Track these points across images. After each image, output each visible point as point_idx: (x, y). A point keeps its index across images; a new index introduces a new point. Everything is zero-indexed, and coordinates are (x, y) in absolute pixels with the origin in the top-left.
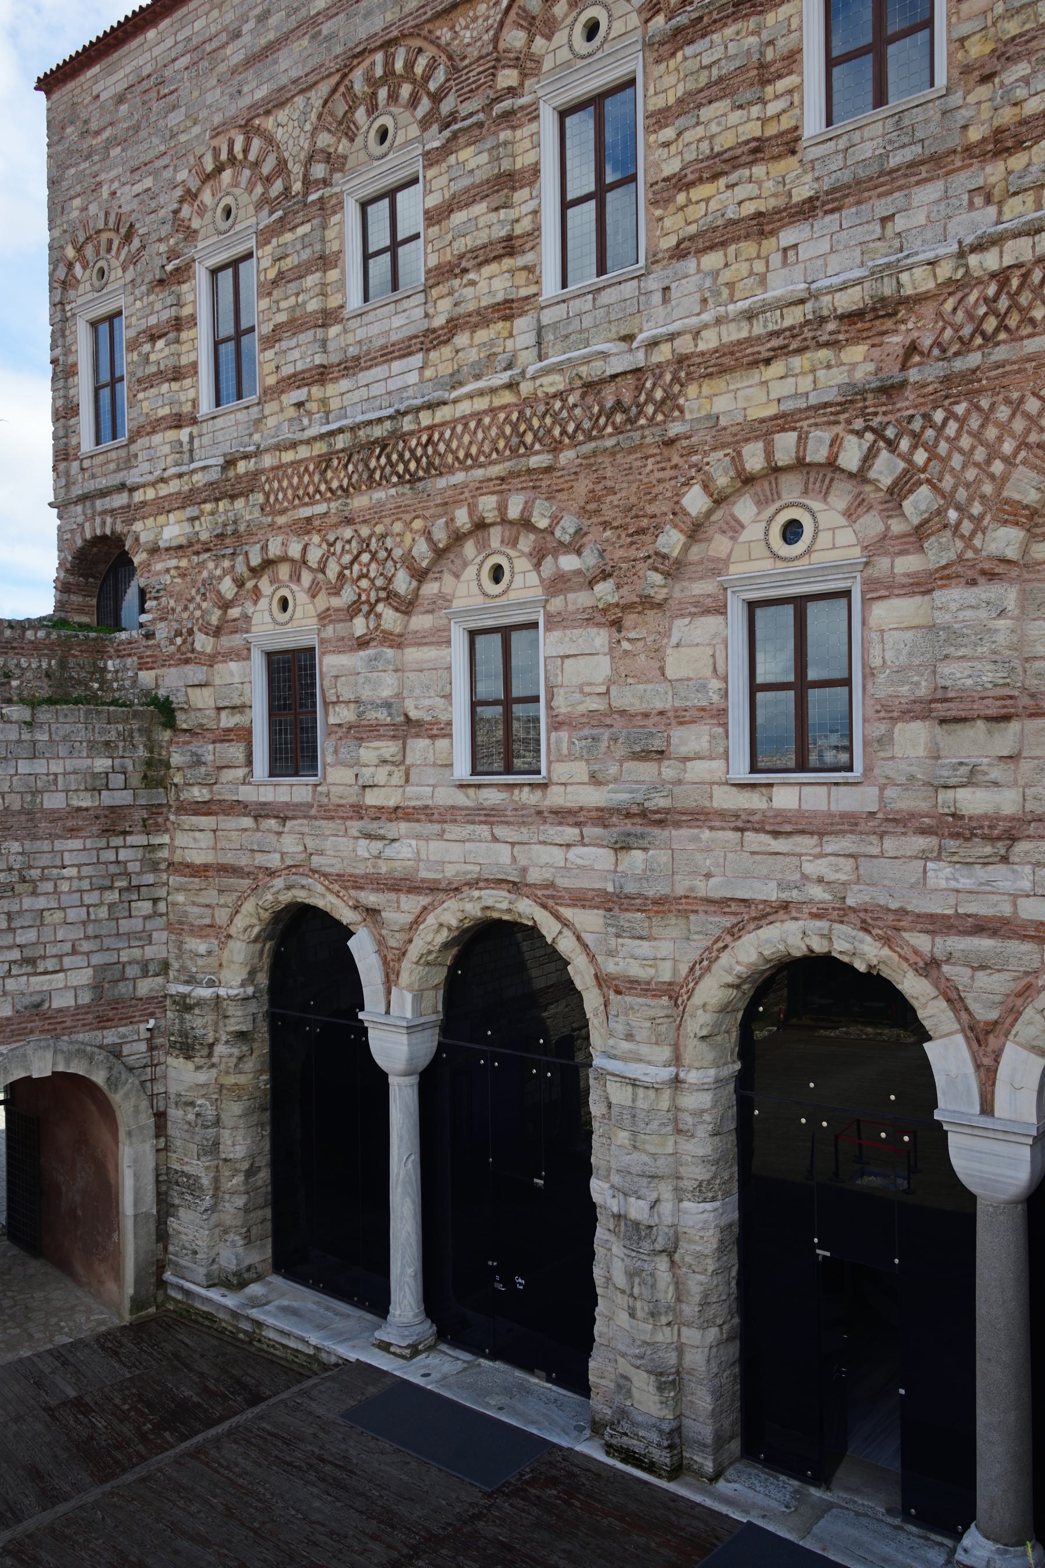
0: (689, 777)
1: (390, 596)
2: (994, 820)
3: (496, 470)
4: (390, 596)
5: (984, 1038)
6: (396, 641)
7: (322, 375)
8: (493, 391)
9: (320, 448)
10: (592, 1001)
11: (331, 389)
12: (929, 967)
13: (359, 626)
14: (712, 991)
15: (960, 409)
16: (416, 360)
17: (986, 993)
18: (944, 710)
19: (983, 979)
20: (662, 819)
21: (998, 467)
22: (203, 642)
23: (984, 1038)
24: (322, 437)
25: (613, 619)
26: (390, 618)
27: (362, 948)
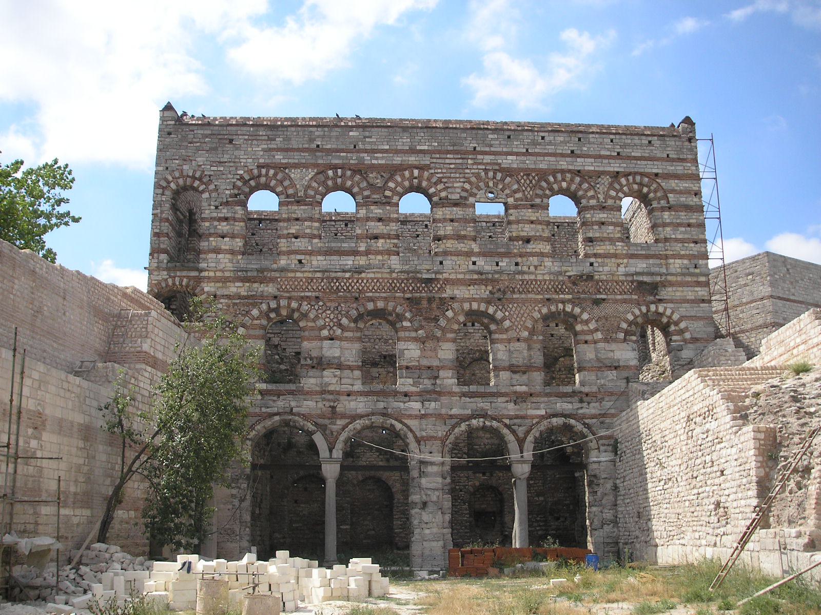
0: (445, 383)
1: (340, 325)
2: (525, 393)
3: (384, 295)
4: (340, 325)
5: (521, 442)
6: (340, 339)
7: (310, 253)
8: (382, 273)
9: (310, 275)
10: (413, 445)
11: (313, 258)
12: (508, 427)
13: (325, 333)
14: (452, 438)
15: (515, 305)
16: (352, 258)
17: (521, 431)
18: (513, 369)
19: (521, 428)
20: (440, 394)
21: (523, 319)
22: (241, 331)
23: (521, 442)
24: (310, 272)
25: (422, 341)
26: (339, 332)
27: (318, 439)
